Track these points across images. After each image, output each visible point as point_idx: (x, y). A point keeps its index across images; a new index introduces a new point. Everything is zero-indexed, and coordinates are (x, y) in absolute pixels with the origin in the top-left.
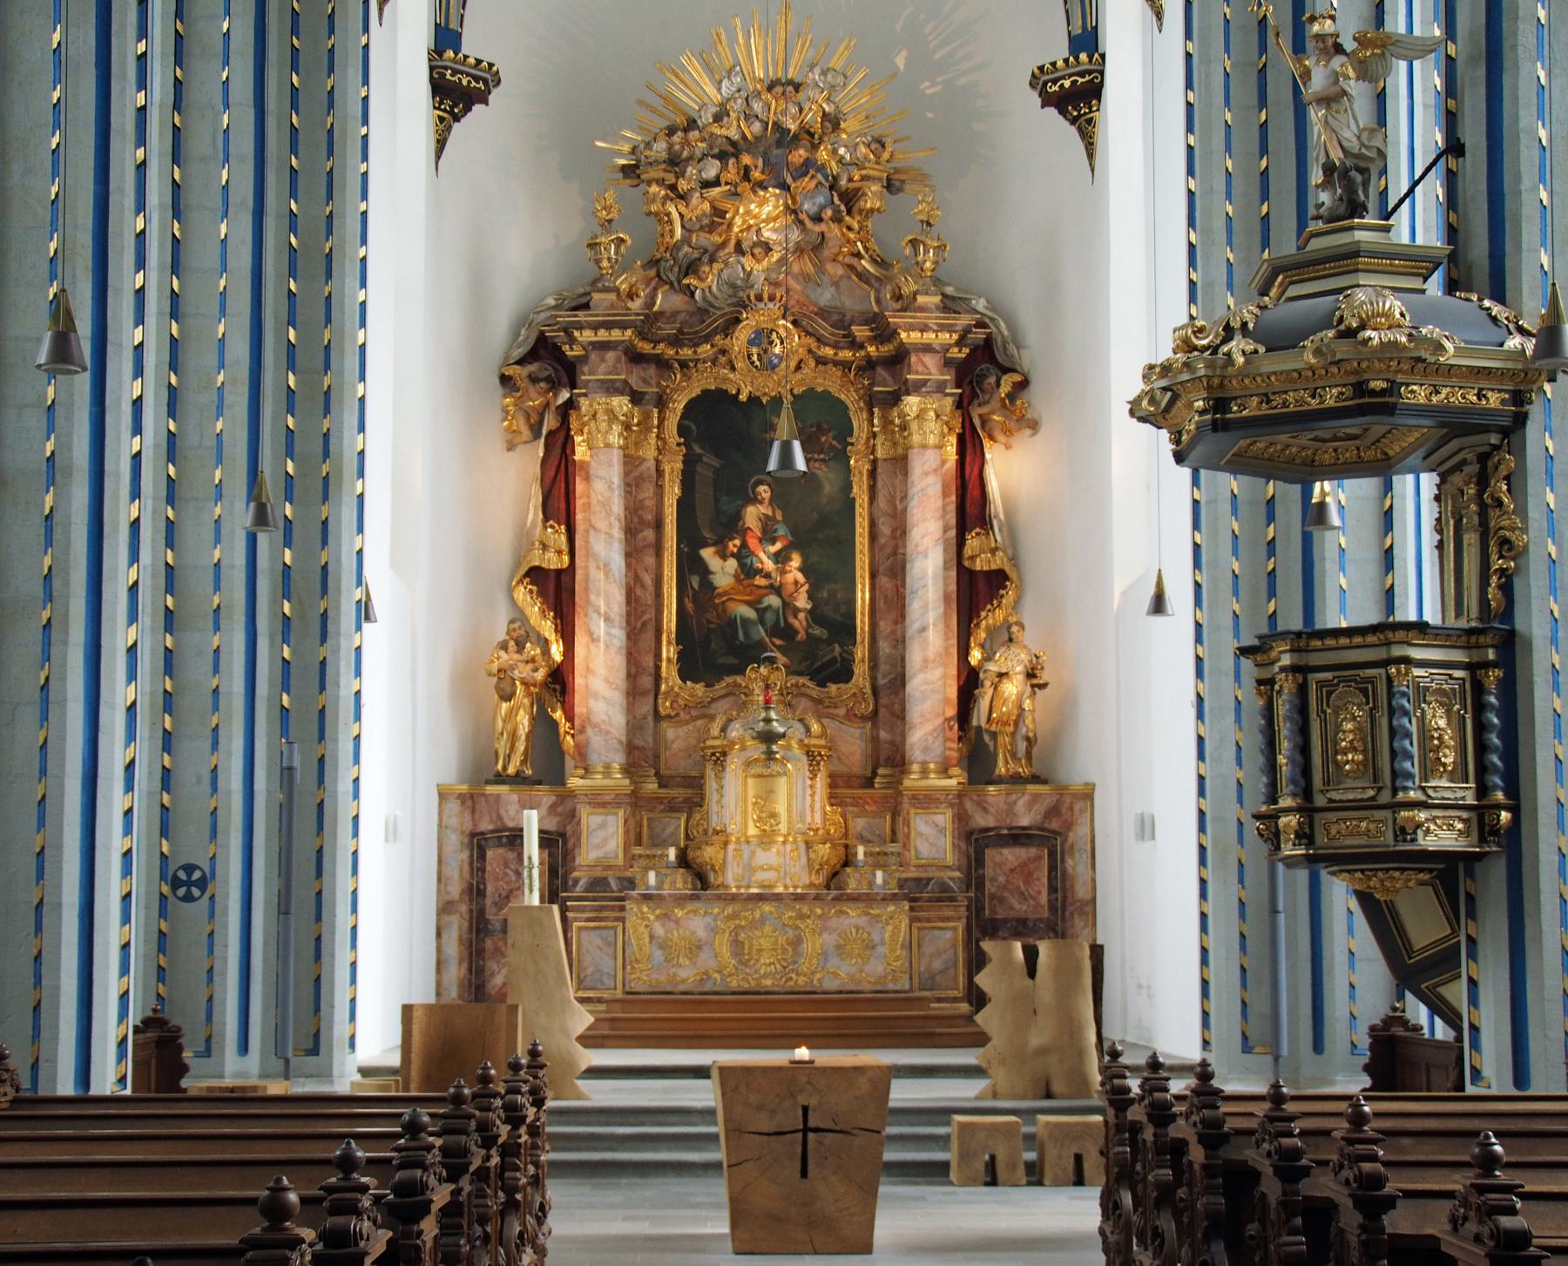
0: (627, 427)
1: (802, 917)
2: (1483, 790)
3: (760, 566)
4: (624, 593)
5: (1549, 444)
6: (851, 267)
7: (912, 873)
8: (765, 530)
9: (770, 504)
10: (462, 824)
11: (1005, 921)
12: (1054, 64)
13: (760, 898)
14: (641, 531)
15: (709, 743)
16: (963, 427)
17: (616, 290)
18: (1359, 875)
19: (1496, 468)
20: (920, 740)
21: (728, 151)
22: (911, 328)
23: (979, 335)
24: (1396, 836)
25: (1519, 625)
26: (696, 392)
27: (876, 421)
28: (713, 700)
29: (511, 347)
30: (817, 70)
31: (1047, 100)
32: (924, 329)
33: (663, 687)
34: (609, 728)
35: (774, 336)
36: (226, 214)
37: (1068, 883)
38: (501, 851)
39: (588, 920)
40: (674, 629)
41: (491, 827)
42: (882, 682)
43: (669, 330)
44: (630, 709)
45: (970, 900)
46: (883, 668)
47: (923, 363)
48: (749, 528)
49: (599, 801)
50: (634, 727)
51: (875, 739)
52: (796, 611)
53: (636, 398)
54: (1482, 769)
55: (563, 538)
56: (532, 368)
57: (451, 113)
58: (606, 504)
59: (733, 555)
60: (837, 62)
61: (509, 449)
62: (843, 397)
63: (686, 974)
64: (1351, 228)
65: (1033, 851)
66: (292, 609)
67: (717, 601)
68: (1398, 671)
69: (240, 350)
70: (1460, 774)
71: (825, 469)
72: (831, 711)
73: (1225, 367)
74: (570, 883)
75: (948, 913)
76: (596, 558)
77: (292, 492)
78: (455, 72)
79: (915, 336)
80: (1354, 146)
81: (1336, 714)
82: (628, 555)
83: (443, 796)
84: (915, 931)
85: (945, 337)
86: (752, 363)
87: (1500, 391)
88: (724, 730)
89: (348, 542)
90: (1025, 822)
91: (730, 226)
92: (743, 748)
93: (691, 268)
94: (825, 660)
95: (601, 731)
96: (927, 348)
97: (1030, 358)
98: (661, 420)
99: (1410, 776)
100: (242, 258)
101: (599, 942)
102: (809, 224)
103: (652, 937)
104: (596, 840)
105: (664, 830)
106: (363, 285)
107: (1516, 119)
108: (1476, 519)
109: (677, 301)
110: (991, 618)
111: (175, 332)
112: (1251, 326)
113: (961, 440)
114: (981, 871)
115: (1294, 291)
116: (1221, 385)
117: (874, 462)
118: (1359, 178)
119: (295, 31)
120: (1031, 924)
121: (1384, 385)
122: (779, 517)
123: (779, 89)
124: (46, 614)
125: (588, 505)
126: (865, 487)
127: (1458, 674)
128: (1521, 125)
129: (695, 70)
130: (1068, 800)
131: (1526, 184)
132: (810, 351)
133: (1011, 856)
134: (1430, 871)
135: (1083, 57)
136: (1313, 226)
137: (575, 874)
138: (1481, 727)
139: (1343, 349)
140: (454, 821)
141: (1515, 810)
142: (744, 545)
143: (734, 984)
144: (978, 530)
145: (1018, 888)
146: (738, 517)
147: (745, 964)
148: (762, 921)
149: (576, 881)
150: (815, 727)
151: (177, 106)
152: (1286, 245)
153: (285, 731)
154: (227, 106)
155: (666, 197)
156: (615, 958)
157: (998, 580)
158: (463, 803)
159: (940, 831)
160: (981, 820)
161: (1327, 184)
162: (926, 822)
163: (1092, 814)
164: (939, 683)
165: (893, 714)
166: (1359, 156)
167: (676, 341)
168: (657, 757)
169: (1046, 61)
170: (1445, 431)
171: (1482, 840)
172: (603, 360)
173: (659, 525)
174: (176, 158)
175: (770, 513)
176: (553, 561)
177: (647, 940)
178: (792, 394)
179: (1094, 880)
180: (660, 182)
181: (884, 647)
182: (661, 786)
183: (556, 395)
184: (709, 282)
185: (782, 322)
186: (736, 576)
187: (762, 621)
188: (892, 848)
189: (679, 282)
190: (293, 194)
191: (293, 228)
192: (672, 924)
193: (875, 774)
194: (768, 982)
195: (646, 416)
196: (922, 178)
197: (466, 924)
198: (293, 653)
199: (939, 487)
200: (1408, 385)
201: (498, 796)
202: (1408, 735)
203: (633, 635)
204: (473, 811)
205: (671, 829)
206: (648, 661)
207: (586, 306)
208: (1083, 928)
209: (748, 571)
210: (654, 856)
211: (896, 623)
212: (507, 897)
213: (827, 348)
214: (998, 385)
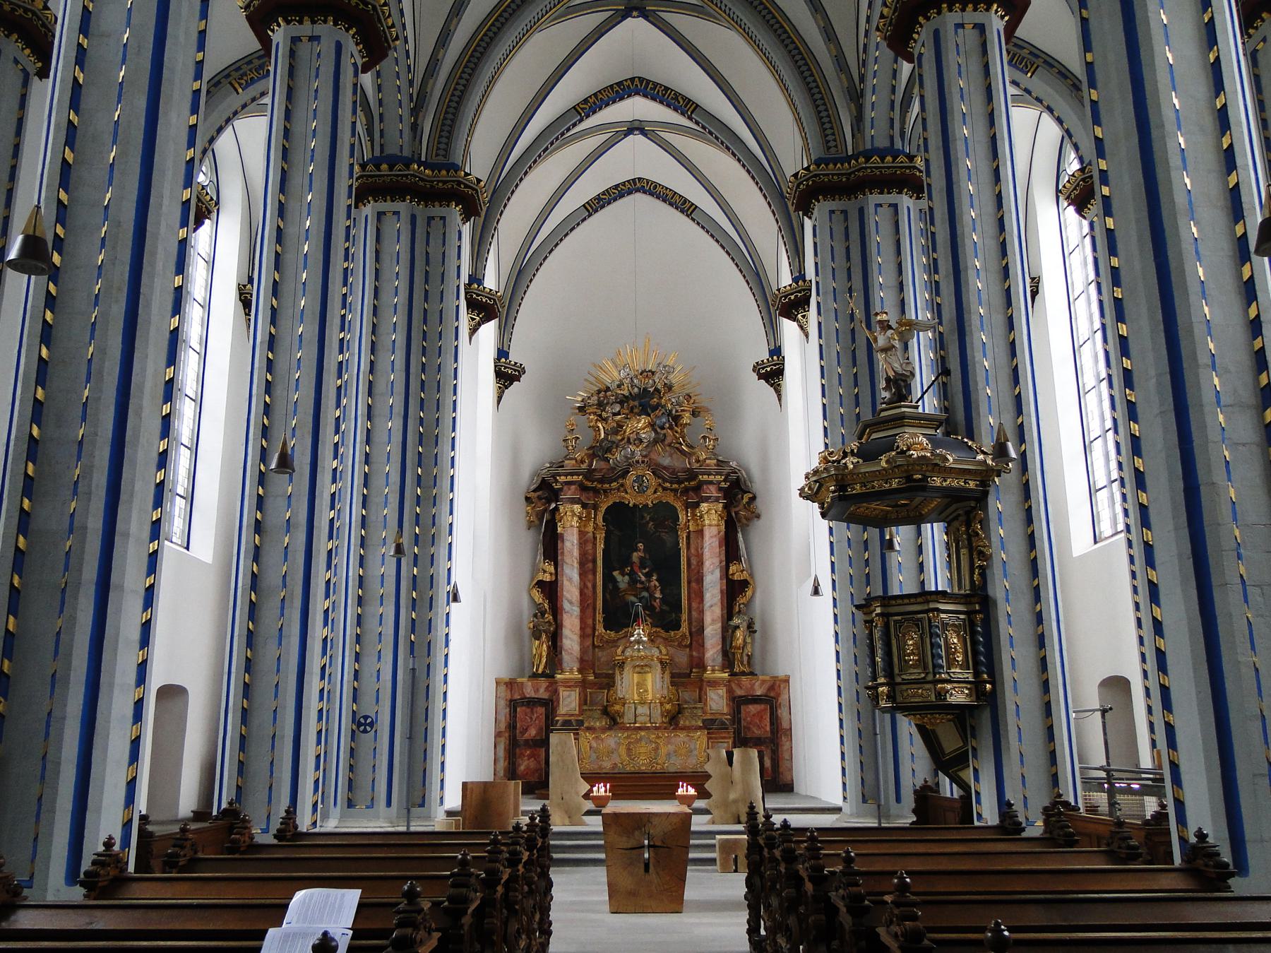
0: (580, 518)
1: (658, 737)
2: (977, 674)
5: (999, 506)
6: (677, 448)
8: (641, 562)
12: (763, 361)
13: (639, 728)
15: (617, 658)
17: (576, 459)
18: (918, 716)
19: (975, 517)
21: (622, 401)
22: (703, 474)
23: (734, 476)
24: (936, 697)
25: (990, 592)
26: (611, 503)
28: (619, 639)
29: (530, 486)
30: (661, 366)
31: (761, 377)
32: (709, 474)
33: (597, 633)
36: (391, 419)
38: (524, 708)
42: (693, 630)
43: (598, 475)
44: (582, 644)
45: (734, 728)
46: (694, 624)
49: (568, 684)
50: (583, 651)
51: (691, 656)
53: (584, 506)
54: (976, 663)
55: (553, 568)
57: (504, 385)
58: (571, 552)
59: (627, 574)
60: (670, 362)
64: (900, 407)
65: (763, 706)
68: (934, 614)
69: (395, 478)
70: (965, 666)
73: (843, 470)
78: (505, 368)
79: (705, 477)
80: (899, 370)
81: (904, 636)
83: (497, 683)
84: (710, 744)
85: (718, 478)
87: (975, 480)
88: (623, 652)
89: (442, 564)
91: (625, 432)
92: (632, 660)
93: (609, 450)
96: (711, 483)
97: (757, 487)
98: (595, 515)
99: (942, 667)
100: (397, 437)
102: (659, 430)
103: (591, 748)
106: (453, 449)
107: (974, 357)
108: (966, 542)
109: (603, 465)
110: (742, 600)
111: (366, 471)
112: (855, 451)
113: (726, 522)
115: (874, 436)
116: (842, 479)
117: (689, 533)
118: (902, 384)
119: (424, 339)
121: (920, 477)
122: (647, 557)
123: (645, 374)
124: (283, 594)
125: (563, 553)
127: (962, 617)
128: (976, 359)
129: (609, 366)
130: (778, 683)
131: (980, 385)
132: (660, 485)
133: (753, 709)
134: (953, 714)
135: (775, 358)
136: (880, 407)
138: (974, 643)
139: (900, 461)
140: (503, 695)
141: (993, 683)
142: (632, 570)
146: (630, 557)
147: (633, 760)
148: (641, 739)
150: (664, 651)
151: (371, 372)
152: (867, 416)
153: (412, 652)
154: (393, 371)
155: (597, 420)
157: (744, 584)
160: (739, 692)
161: (887, 388)
165: (699, 645)
166: (903, 375)
167: (602, 481)
169: (759, 360)
170: (949, 500)
171: (978, 699)
172: (569, 489)
173: (594, 561)
174: (370, 394)
176: (547, 578)
179: (790, 720)
180: (595, 413)
181: (694, 614)
182: (595, 678)
183: (550, 506)
184: (618, 456)
186: (628, 583)
188: (699, 705)
190: (422, 409)
191: (421, 424)
193: (691, 672)
194: (644, 768)
195: (589, 514)
196: (707, 410)
198: (417, 616)
199: (717, 542)
200: (931, 477)
202: (940, 647)
203: (583, 610)
206: (590, 622)
207: (563, 466)
209: (634, 580)
211: (699, 603)
214: (743, 499)
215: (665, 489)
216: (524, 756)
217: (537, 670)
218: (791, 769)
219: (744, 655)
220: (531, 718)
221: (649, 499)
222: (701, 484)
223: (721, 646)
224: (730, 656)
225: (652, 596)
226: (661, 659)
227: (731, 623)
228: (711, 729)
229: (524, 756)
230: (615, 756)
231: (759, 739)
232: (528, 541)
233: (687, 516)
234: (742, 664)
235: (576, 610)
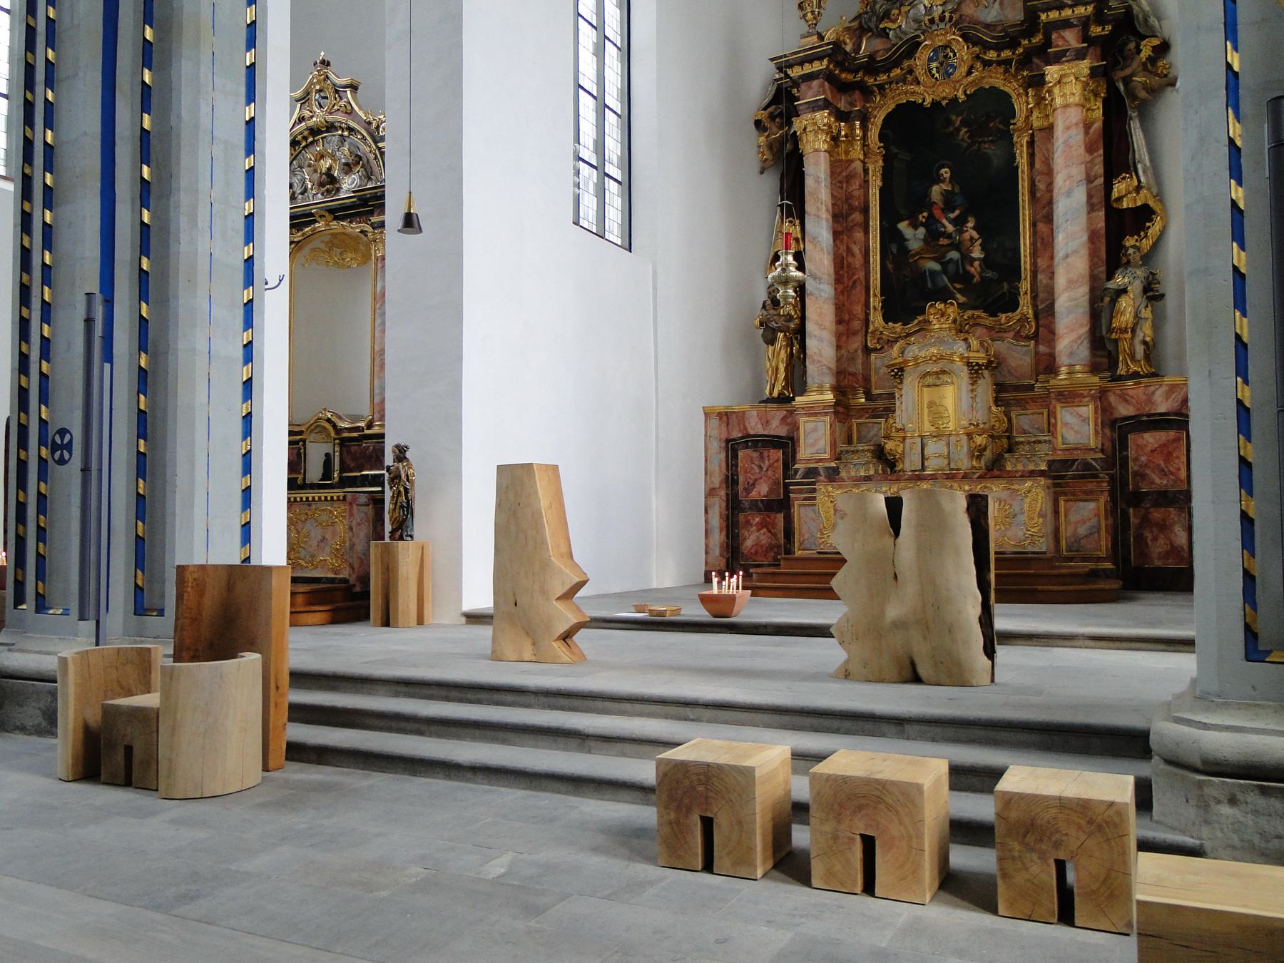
0: (835, 139)
3: (942, 229)
4: (831, 257)
7: (1060, 456)
9: (950, 182)
10: (720, 434)
11: (1147, 493)
14: (851, 215)
16: (1108, 92)
20: (1065, 347)
26: (891, 106)
27: (1030, 100)
28: (908, 335)
33: (871, 328)
34: (820, 359)
38: (749, 451)
39: (805, 499)
41: (739, 435)
45: (1112, 477)
46: (1042, 295)
47: (1063, 38)
49: (811, 411)
51: (1037, 353)
53: (841, 116)
55: (798, 228)
56: (770, 109)
59: (922, 224)
61: (762, 173)
62: (1007, 89)
66: (151, 173)
67: (911, 261)
72: (1002, 334)
75: (1090, 486)
77: (151, 58)
79: (1054, 15)
82: (836, 235)
84: (1062, 503)
86: (933, 76)
90: (1162, 409)
92: (917, 365)
94: (996, 296)
96: (1066, 24)
103: (835, 510)
104: (810, 441)
105: (869, 432)
109: (878, 44)
113: (1105, 101)
114: (1125, 453)
120: (1171, 496)
122: (957, 190)
126: (1025, 156)
133: (1151, 439)
140: (715, 433)
142: (931, 216)
144: (1124, 175)
145: (1159, 465)
146: (927, 194)
149: (796, 471)
157: (1143, 215)
158: (720, 419)
159: (1084, 421)
160: (1124, 410)
162: (1071, 414)
164: (1083, 299)
168: (867, 380)
172: (810, 88)
173: (865, 210)
175: (950, 189)
177: (832, 512)
178: (966, 94)
185: (954, 37)
186: (925, 240)
187: (945, 271)
189: (877, 27)
195: (852, 129)
197: (724, 504)
198: (152, 217)
201: (744, 412)
204: (728, 425)
206: (858, 310)
209: (934, 233)
210: (857, 451)
212: (754, 484)
213: (991, 51)
214: (1139, 51)
215: (987, 64)
216: (751, 525)
217: (771, 394)
220: (760, 467)
221: (957, 88)
223: (1085, 329)
224: (1110, 347)
225: (967, 259)
226: (968, 358)
227: (1111, 285)
228: (1062, 477)
229: (751, 525)
232: (765, 189)
234: (1133, 357)
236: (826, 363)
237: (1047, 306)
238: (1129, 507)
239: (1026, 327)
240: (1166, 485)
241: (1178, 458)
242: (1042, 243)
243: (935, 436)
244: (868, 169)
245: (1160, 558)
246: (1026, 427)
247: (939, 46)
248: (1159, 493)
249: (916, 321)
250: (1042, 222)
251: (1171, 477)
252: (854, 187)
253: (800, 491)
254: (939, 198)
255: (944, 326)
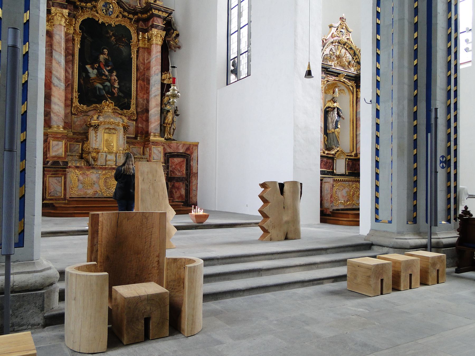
3: (104, 73)
9: (107, 55)
11: (174, 178)
22: (155, 9)
26: (86, 17)
28: (89, 111)
32: (159, 10)
33: (74, 105)
34: (60, 115)
35: (111, 5)
37: (191, 168)
40: (77, 88)
46: (140, 106)
48: (101, 61)
50: (66, 116)
52: (115, 88)
58: (59, 43)
59: (96, 68)
62: (130, 29)
63: (90, 192)
65: (182, 159)
71: (124, 48)
74: (46, 162)
76: (55, 59)
88: (98, 118)
90: (181, 151)
92: (104, 124)
94: (123, 103)
95: (57, 115)
96: (159, 16)
101: (56, 181)
103: (78, 180)
104: (55, 149)
114: (168, 164)
117: (138, 48)
122: (110, 60)
130: (192, 146)
133: (177, 160)
137: (47, 160)
142: (99, 66)
143: (105, 195)
144: (166, 72)
146: (98, 57)
147: (109, 189)
156: (61, 186)
160: (169, 150)
162: (156, 150)
163: (198, 150)
175: (107, 58)
178: (115, 24)
179: (197, 168)
186: (97, 75)
187: (104, 89)
192: (85, 176)
205: (77, 147)
208: (195, 180)
209: (100, 74)
210: (73, 155)
214: (173, 33)
215: (124, 16)
218: (196, 196)
219: (172, 128)
222: (153, 15)
223: (159, 122)
225: (112, 86)
230: (96, 186)
231: (179, 178)
233: (138, 37)
234: (170, 134)
235: (62, 86)
236: (62, 117)
237: (142, 110)
238: (168, 182)
239: (132, 116)
240: (180, 175)
241: (183, 167)
242: (141, 88)
243: (111, 153)
244: (75, 39)
245: (177, 198)
246: (135, 152)
247: (108, 2)
248: (178, 178)
249: (92, 106)
250: (141, 80)
251: (181, 173)
252: (70, 45)
253: (50, 171)
254: (103, 60)
255: (110, 111)
